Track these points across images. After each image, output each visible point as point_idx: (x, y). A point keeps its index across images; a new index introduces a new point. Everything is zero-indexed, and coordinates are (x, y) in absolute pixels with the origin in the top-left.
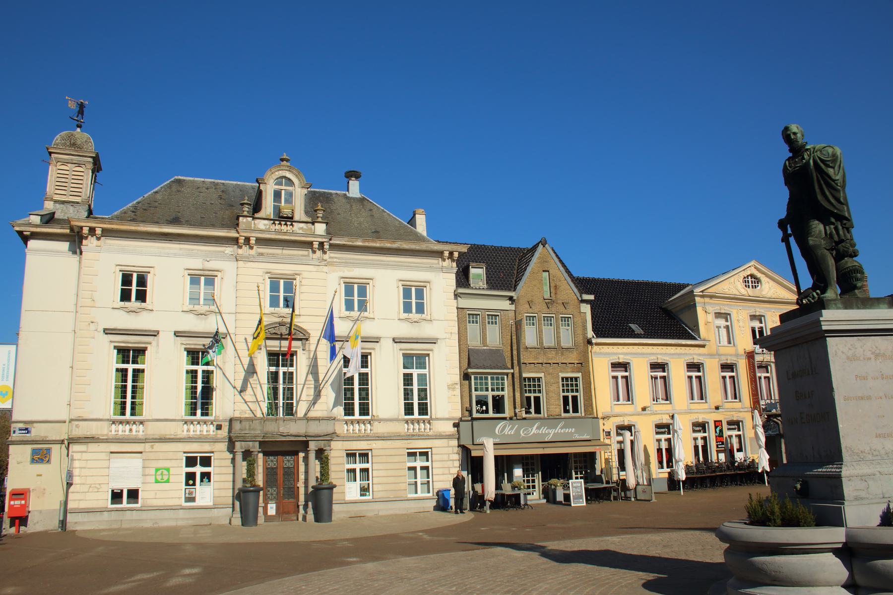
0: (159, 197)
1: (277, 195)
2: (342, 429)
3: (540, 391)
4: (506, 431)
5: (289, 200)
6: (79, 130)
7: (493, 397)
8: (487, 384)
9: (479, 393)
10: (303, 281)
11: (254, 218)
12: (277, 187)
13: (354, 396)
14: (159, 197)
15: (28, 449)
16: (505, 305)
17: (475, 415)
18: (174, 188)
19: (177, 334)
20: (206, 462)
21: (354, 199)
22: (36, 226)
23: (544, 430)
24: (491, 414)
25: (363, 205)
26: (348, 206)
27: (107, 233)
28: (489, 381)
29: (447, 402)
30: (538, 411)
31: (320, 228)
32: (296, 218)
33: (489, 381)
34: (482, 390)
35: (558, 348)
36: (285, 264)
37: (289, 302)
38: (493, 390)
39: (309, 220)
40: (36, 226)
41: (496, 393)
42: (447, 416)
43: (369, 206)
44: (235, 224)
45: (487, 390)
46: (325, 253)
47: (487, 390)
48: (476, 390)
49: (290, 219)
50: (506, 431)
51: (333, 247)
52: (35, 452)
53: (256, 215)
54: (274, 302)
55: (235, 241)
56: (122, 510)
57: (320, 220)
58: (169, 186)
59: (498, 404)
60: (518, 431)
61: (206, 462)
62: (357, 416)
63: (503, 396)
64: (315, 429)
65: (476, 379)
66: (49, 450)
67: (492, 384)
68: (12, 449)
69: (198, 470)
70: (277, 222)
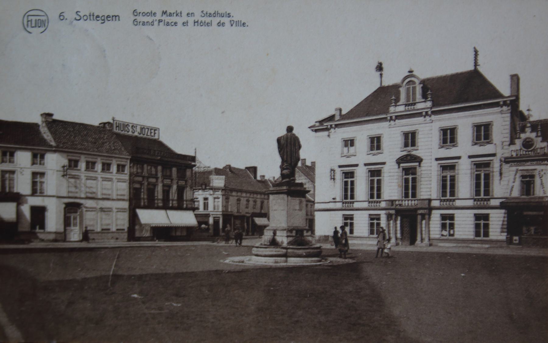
10: (420, 133)
13: (448, 186)
19: (366, 165)
22: (318, 126)
27: (337, 126)
31: (429, 104)
36: (408, 125)
37: (413, 144)
39: (423, 100)
40: (318, 126)
42: (500, 196)
44: (387, 112)
46: (430, 116)
51: (434, 113)
53: (398, 104)
55: (385, 119)
68: (316, 213)
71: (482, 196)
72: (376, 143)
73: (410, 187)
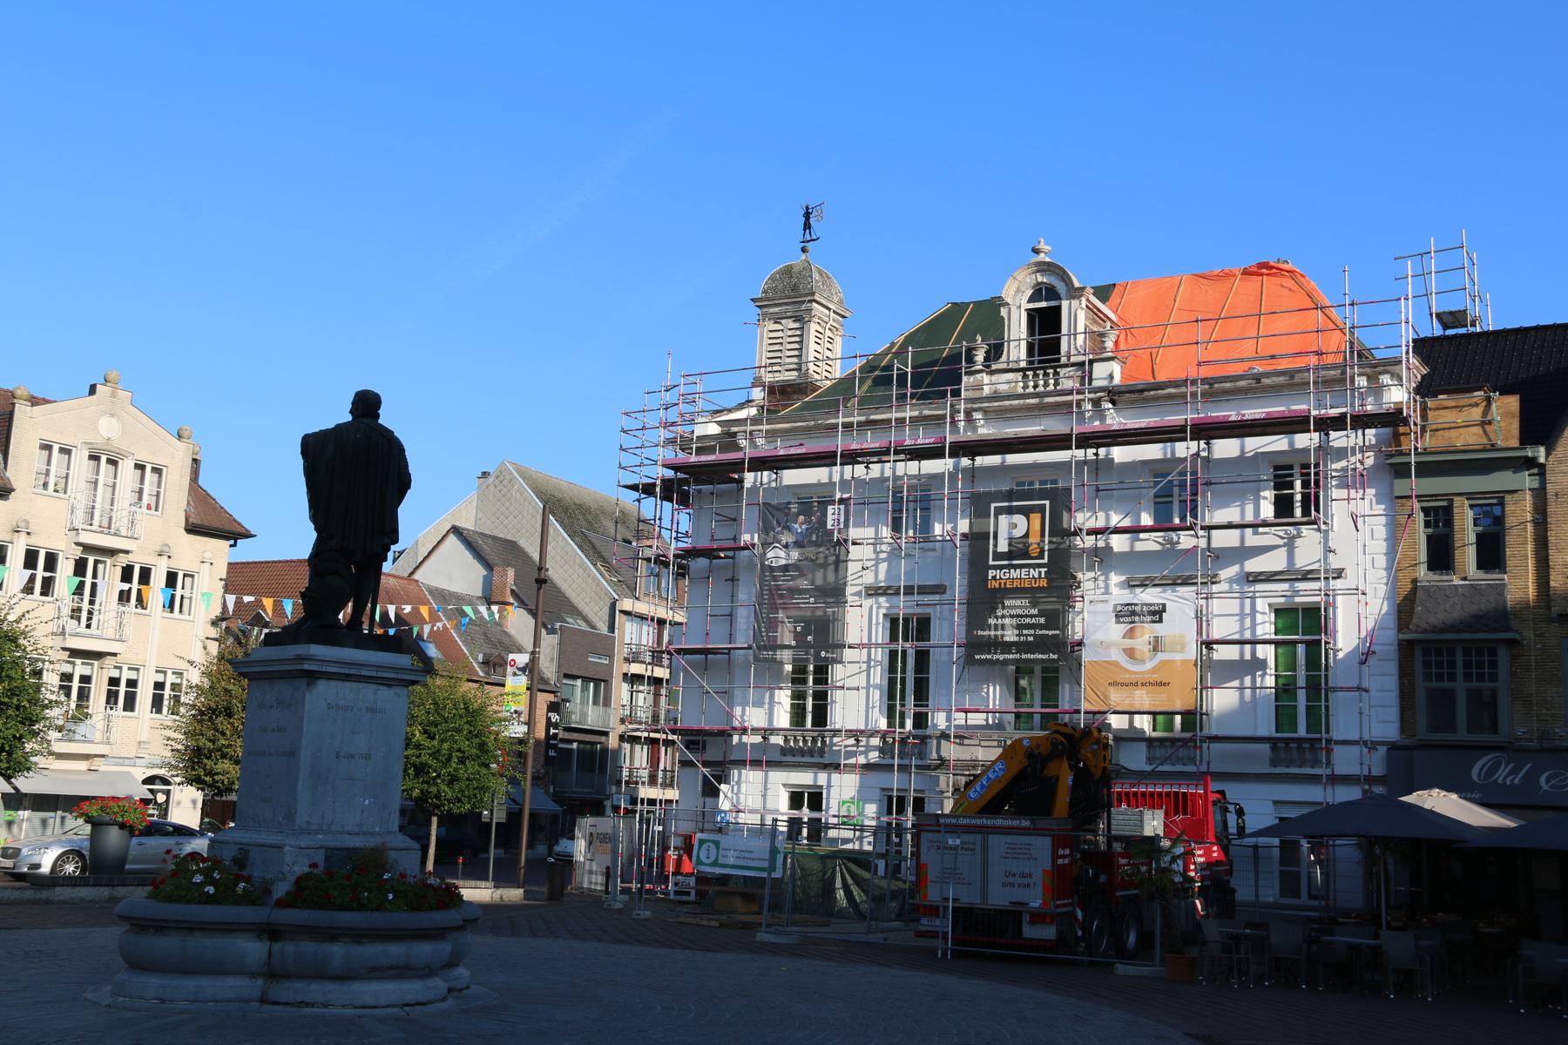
4: (1501, 775)
6: (803, 257)
7: (1469, 692)
8: (1452, 665)
11: (992, 373)
24: (1462, 734)
28: (1459, 659)
32: (1064, 360)
33: (1459, 659)
34: (1440, 678)
38: (1468, 677)
41: (1475, 684)
47: (1452, 677)
48: (1428, 677)
50: (1501, 775)
60: (1532, 777)
67: (1467, 665)
70: (1030, 373)
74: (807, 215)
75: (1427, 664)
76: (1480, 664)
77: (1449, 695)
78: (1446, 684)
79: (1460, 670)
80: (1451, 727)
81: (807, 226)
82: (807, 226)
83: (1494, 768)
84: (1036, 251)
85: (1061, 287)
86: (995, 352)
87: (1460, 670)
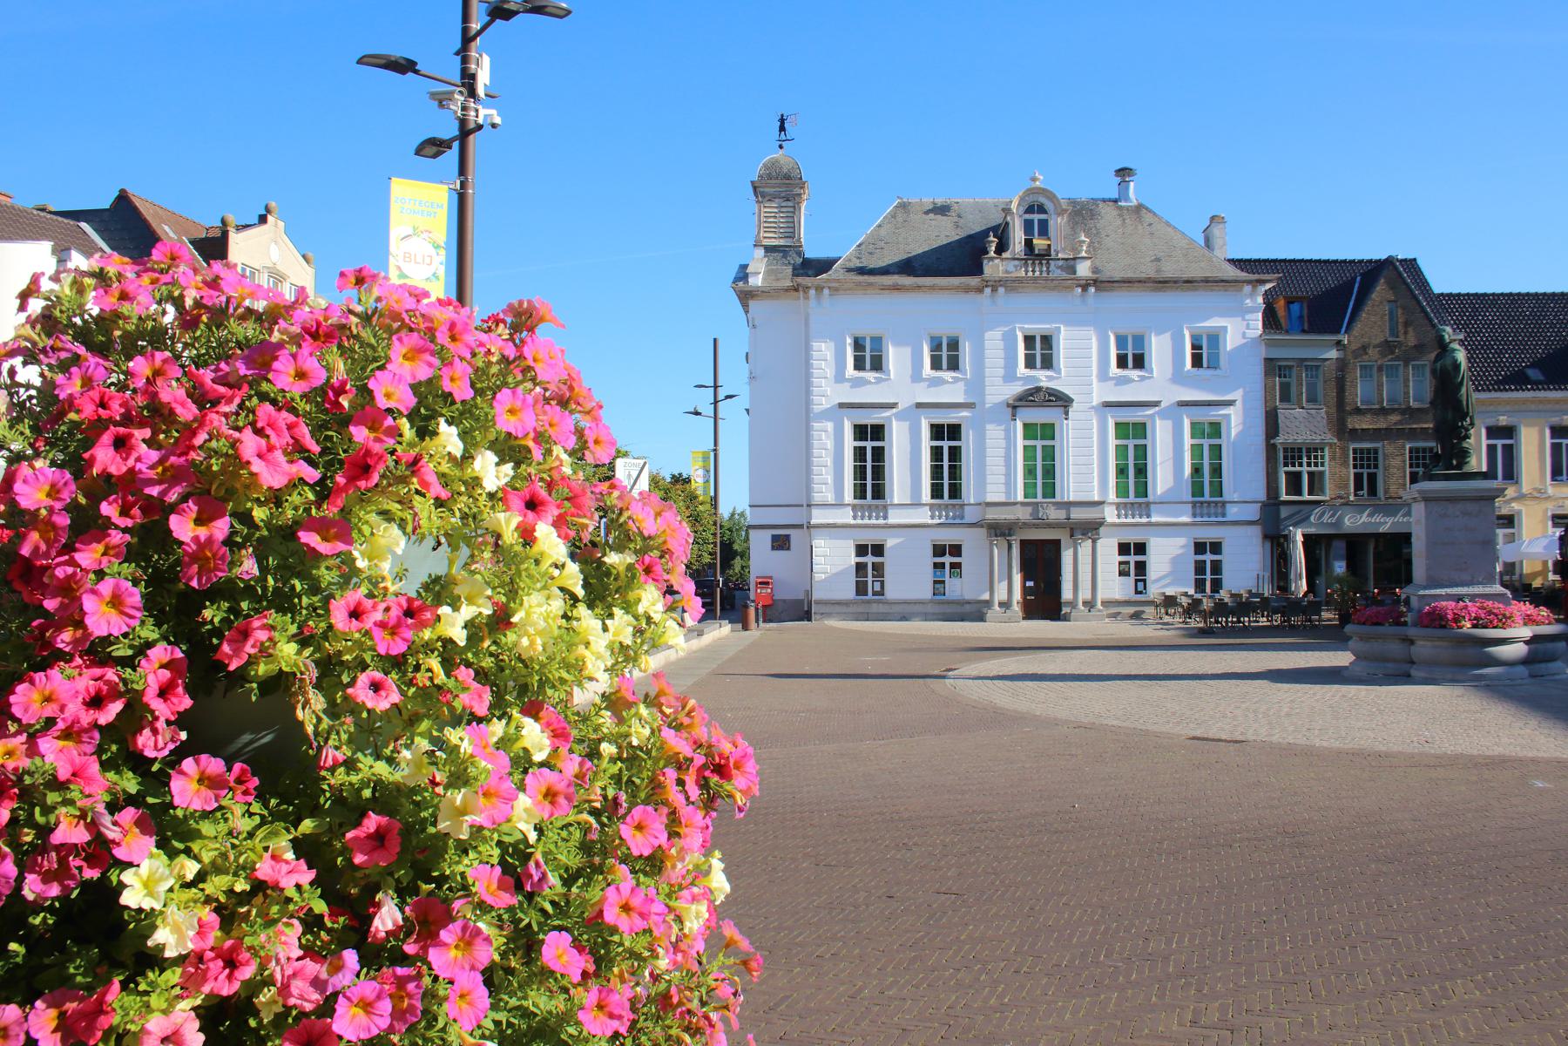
0: (883, 232)
1: (1028, 226)
2: (1110, 515)
3: (1376, 467)
4: (1325, 519)
5: (1044, 232)
9: (1290, 469)
12: (1028, 216)
14: (883, 232)
15: (769, 533)
16: (1333, 354)
17: (1284, 497)
18: (900, 219)
20: (956, 550)
21: (1127, 208)
23: (1377, 518)
24: (1306, 497)
25: (1140, 219)
26: (1119, 222)
29: (1245, 483)
30: (1373, 491)
35: (1410, 413)
37: (1048, 363)
41: (1313, 468)
43: (1148, 218)
45: (1301, 465)
47: (1301, 465)
49: (1045, 256)
50: (1326, 516)
52: (775, 538)
53: (1004, 255)
54: (1030, 364)
56: (869, 602)
57: (1084, 254)
58: (893, 215)
59: (1316, 481)
61: (956, 550)
62: (1132, 498)
63: (1322, 474)
64: (1077, 514)
65: (1285, 450)
66: (788, 537)
69: (948, 560)
71: (1207, 497)
72: (947, 355)
73: (1043, 470)
74: (782, 121)
75: (1285, 458)
76: (1293, 457)
77: (1298, 475)
78: (1297, 469)
79: (1305, 460)
80: (1300, 494)
81: (782, 128)
82: (782, 128)
83: (1323, 514)
84: (1034, 179)
85: (1049, 205)
86: (1001, 249)
87: (1305, 460)
